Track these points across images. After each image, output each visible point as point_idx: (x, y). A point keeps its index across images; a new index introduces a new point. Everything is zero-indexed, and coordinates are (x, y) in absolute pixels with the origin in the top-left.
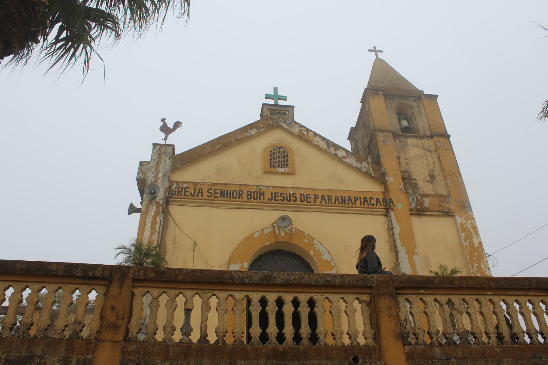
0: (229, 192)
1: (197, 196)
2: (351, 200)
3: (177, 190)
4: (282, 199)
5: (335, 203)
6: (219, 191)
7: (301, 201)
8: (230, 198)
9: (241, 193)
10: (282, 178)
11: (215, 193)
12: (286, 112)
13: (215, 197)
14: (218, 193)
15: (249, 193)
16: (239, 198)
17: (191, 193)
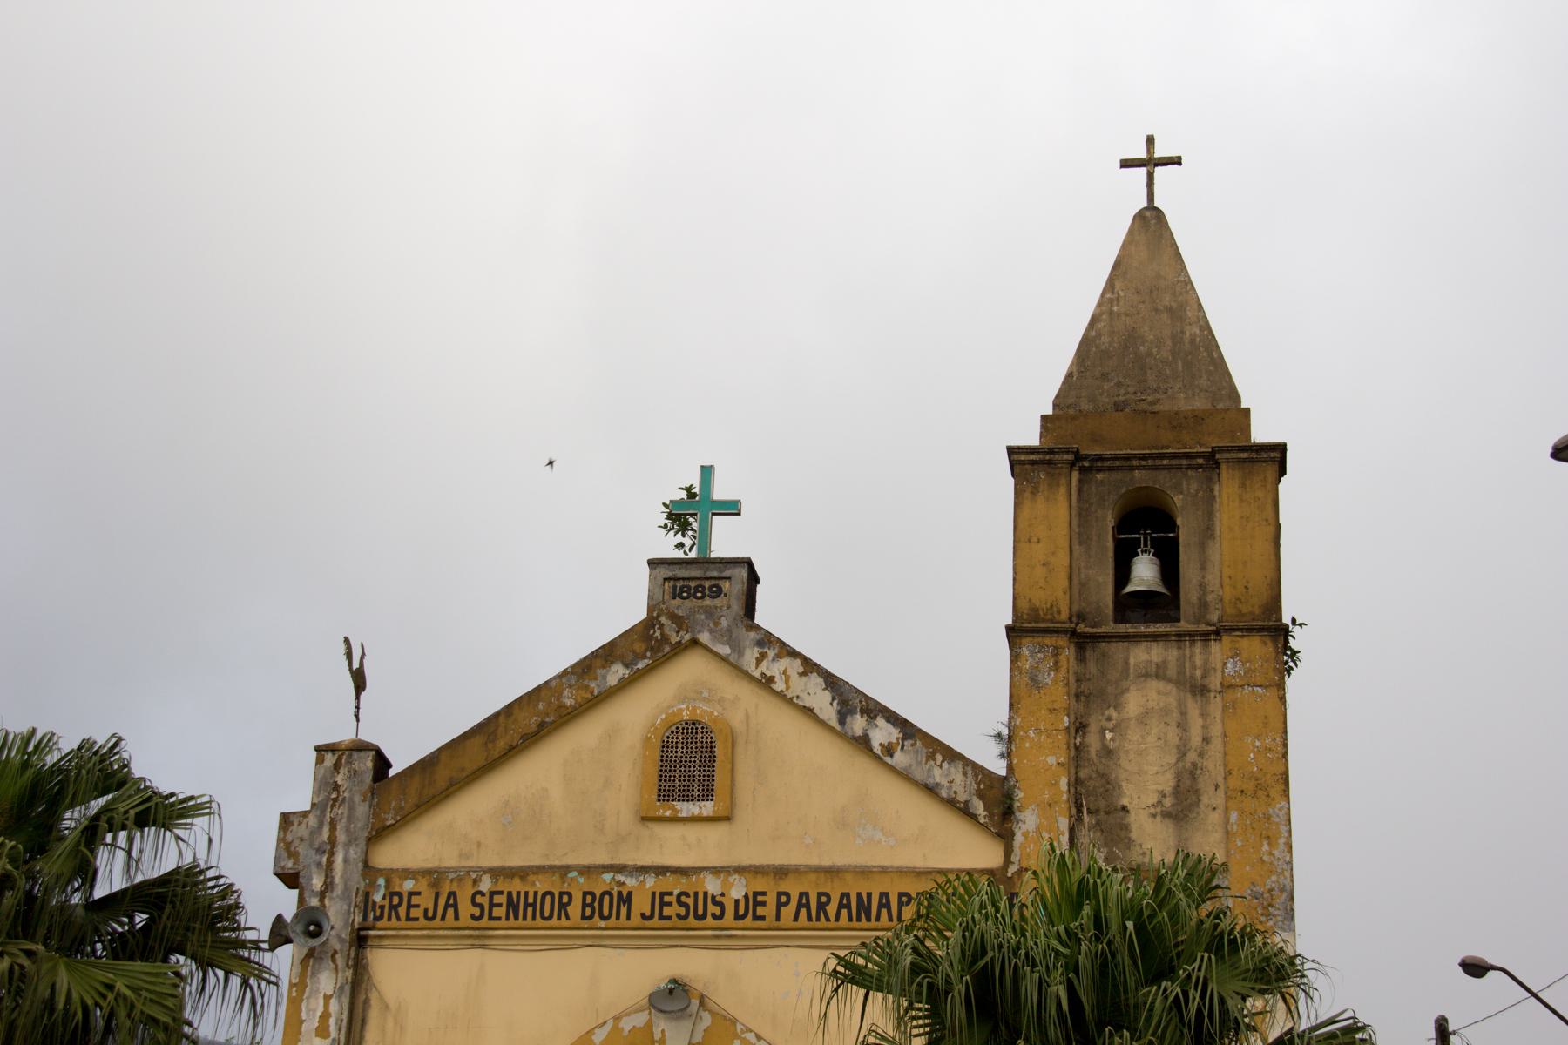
4: (682, 911)
6: (502, 899)
9: (565, 899)
13: (491, 918)
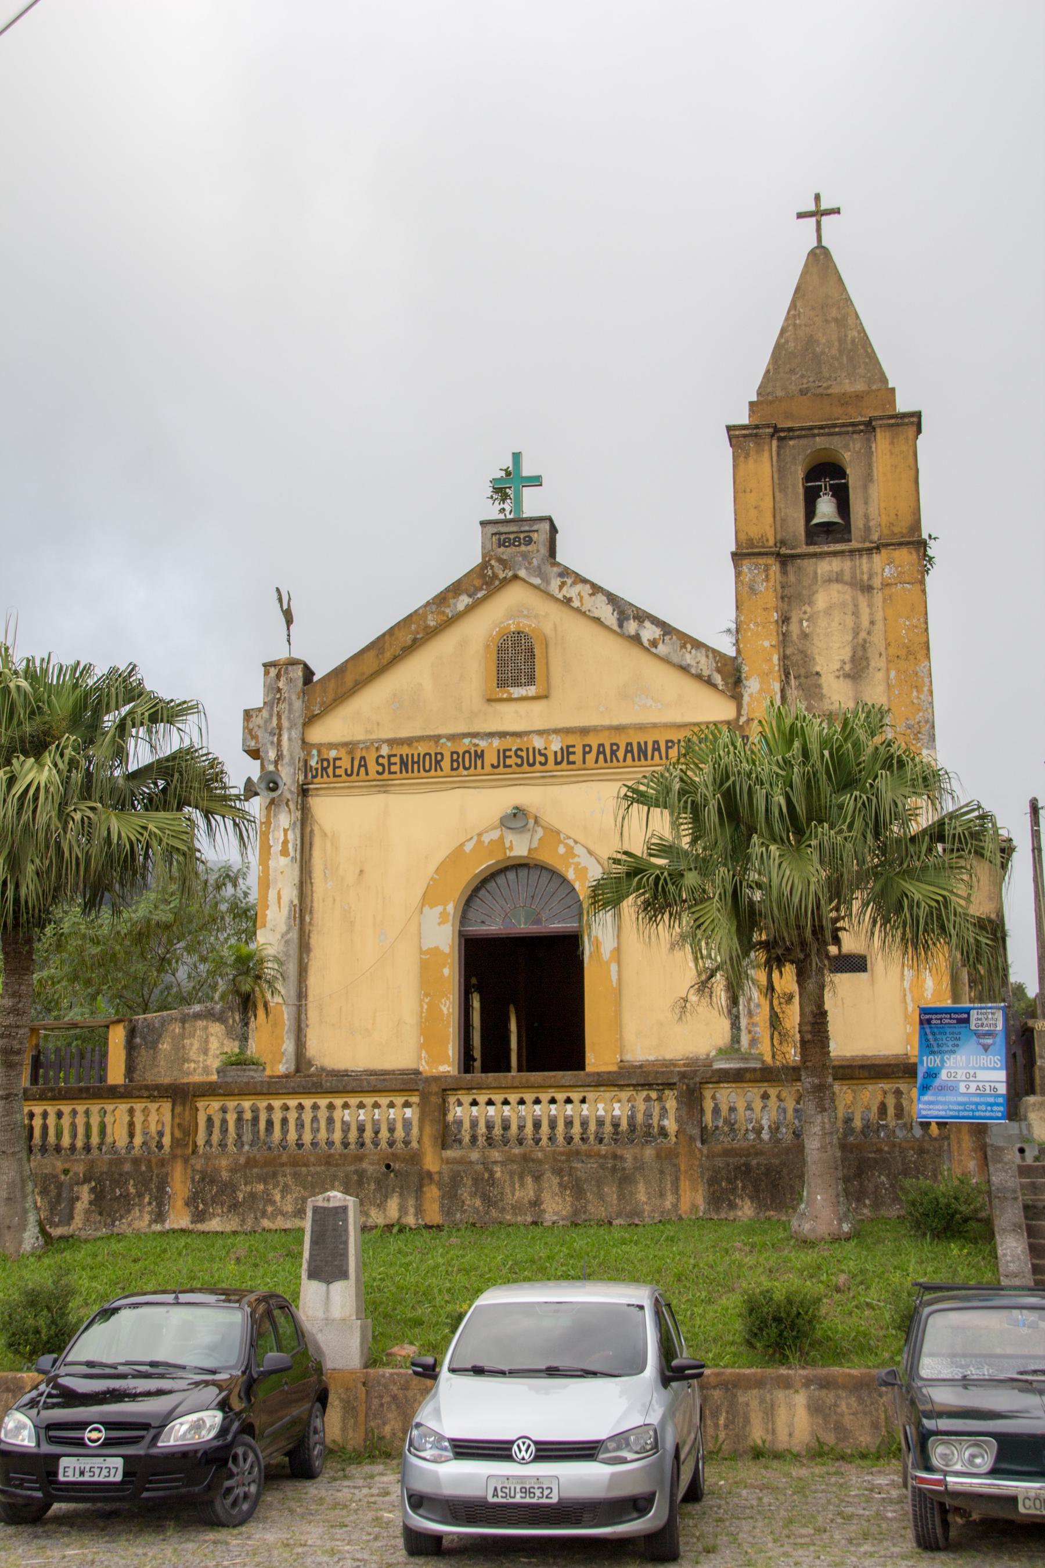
0: (416, 759)
1: (358, 774)
2: (659, 750)
3: (319, 766)
4: (519, 761)
5: (625, 760)
7: (557, 763)
8: (419, 771)
9: (439, 758)
10: (522, 707)
11: (390, 764)
12: (531, 534)
13: (390, 773)
14: (395, 764)
15: (455, 756)
16: (436, 770)
17: (346, 770)
